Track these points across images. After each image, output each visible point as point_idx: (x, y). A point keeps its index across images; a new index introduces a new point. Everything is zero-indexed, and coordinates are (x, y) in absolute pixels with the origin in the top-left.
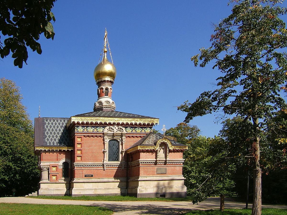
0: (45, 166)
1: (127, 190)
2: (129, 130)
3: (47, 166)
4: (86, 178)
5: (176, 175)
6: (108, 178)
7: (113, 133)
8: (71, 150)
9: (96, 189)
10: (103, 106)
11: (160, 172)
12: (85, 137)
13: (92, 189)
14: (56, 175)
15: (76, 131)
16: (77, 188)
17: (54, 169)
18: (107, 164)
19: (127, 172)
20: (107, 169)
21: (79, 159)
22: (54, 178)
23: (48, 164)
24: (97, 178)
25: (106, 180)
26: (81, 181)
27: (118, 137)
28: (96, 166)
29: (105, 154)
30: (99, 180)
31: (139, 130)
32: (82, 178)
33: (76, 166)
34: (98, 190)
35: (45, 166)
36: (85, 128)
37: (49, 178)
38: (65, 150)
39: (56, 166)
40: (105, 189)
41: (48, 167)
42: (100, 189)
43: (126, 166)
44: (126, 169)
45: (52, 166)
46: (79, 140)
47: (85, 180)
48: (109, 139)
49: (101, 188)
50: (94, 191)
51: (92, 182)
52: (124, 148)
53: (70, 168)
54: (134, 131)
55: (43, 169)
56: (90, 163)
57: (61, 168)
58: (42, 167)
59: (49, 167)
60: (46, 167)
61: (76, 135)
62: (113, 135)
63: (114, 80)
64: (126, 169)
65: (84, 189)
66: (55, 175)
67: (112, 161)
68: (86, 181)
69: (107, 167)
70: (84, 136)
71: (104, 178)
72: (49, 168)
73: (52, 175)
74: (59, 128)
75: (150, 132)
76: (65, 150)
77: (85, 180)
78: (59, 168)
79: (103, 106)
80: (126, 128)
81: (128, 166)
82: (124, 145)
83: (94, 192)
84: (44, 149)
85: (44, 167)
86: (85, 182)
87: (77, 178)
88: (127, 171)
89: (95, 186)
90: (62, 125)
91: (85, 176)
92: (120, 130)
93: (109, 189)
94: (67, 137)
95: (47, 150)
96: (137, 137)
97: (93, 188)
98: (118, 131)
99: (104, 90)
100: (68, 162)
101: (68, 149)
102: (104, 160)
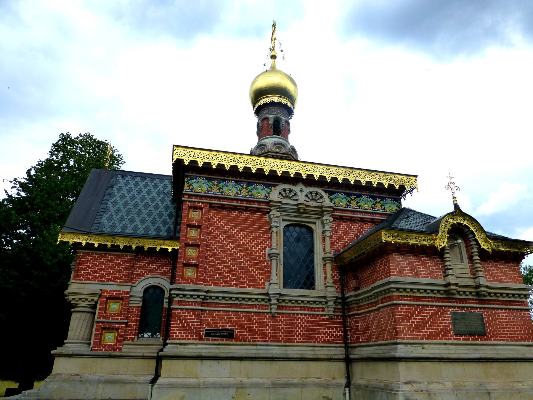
1: (349, 390)
2: (341, 201)
3: (90, 298)
4: (208, 340)
5: (518, 343)
6: (282, 344)
7: (298, 205)
8: (173, 249)
10: (270, 153)
11: (463, 329)
12: (213, 207)
14: (118, 329)
15: (186, 187)
16: (172, 380)
17: (114, 306)
18: (281, 295)
19: (345, 327)
20: (279, 311)
21: (190, 273)
22: (110, 337)
23: (96, 288)
24: (247, 343)
25: (276, 350)
26: (191, 351)
27: (310, 218)
28: (244, 299)
29: (274, 262)
30: (252, 351)
31: (366, 204)
32: (193, 339)
33: (178, 295)
34: (248, 391)
35: (84, 297)
37: (90, 340)
38: (155, 248)
39: (122, 299)
40: (275, 385)
41: (93, 300)
43: (339, 307)
44: (341, 314)
45: (109, 298)
46: (195, 215)
47: (205, 348)
48: (284, 220)
49: (261, 380)
51: (229, 355)
52: (328, 249)
53: (165, 305)
54: (353, 204)
55: (75, 306)
56: (225, 289)
57: (137, 305)
58: (74, 299)
59: (96, 298)
60: (86, 299)
61: (187, 201)
62: (300, 210)
63: (293, 105)
64: (341, 314)
65: (197, 386)
66: (113, 329)
67: (294, 288)
68: (209, 351)
69: (281, 305)
70: (210, 204)
71: (269, 343)
72: (96, 303)
73: (104, 329)
74: (154, 194)
75: (396, 210)
76: (155, 248)
77: (205, 348)
78: (130, 305)
79: (270, 153)
81: (346, 307)
82: (328, 240)
83: (233, 398)
84: (88, 242)
85: (80, 299)
86: (204, 355)
87: (176, 341)
88: (344, 322)
89: (240, 372)
90: (162, 189)
91: (209, 334)
92: (314, 197)
94: (170, 216)
95: (96, 246)
96: (362, 220)
97: (232, 381)
98: (309, 200)
100: (163, 287)
101: (165, 247)
102: (269, 281)
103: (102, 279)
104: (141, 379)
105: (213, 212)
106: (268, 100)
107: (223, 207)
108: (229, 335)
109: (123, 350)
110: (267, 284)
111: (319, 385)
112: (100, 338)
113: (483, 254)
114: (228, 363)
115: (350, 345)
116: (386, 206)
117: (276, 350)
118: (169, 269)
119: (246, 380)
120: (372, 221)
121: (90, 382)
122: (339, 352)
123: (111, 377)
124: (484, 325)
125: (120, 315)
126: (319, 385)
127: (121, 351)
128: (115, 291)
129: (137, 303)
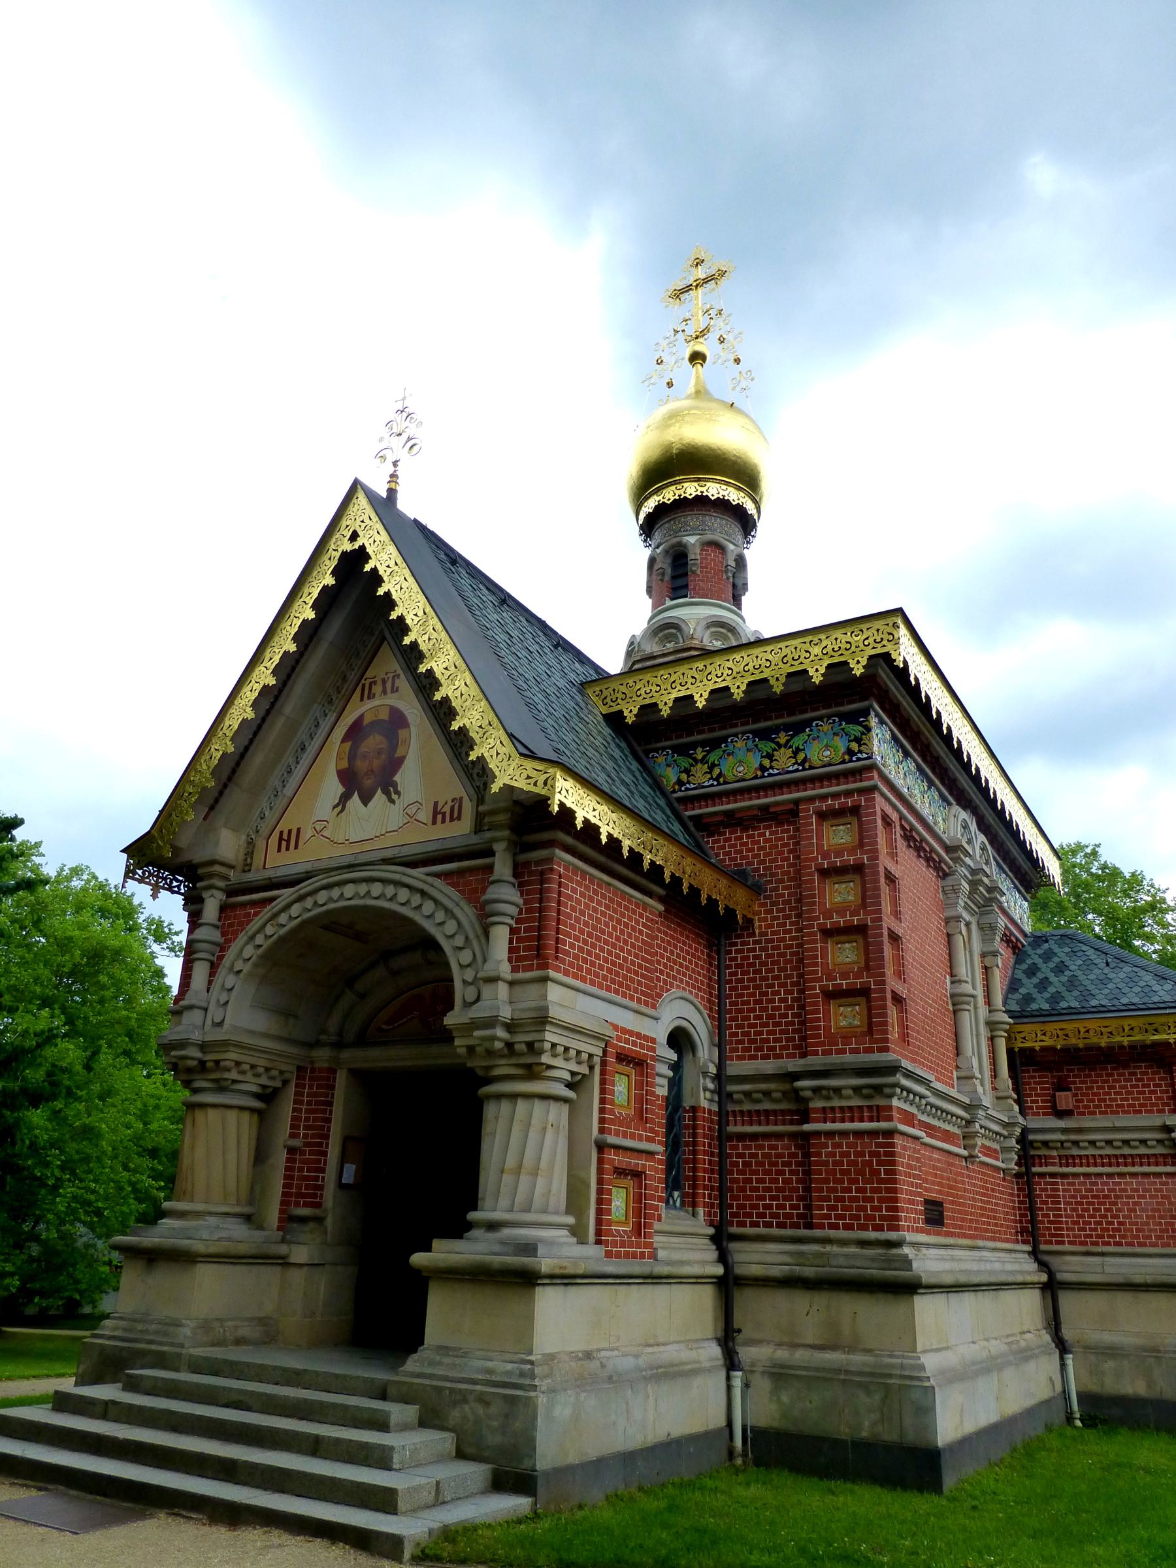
0: (576, 1044)
35: (576, 1044)
106: (691, 489)
109: (661, 1254)
115: (1043, 1247)
122: (1020, 1264)
127: (653, 1256)
128: (631, 1033)
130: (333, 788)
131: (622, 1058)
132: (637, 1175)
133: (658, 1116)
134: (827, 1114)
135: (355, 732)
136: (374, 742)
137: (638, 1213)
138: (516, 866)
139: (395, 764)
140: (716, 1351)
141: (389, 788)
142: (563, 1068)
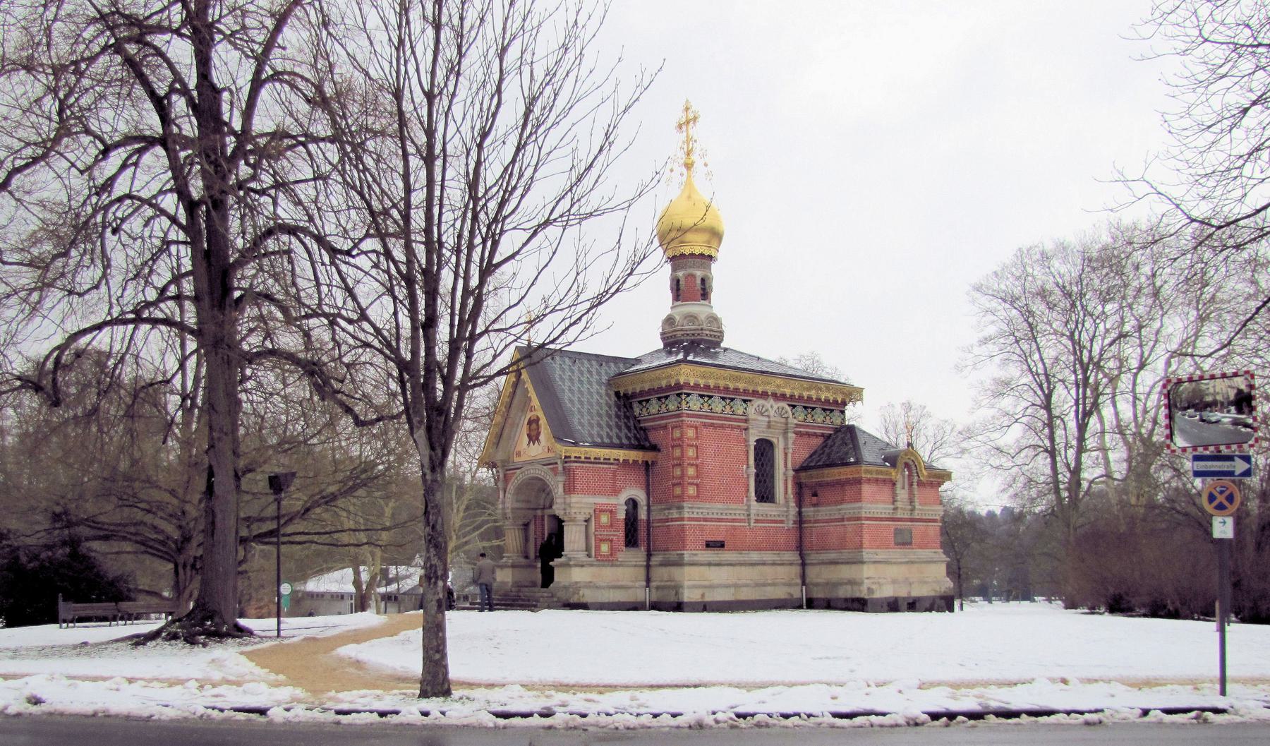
0: (583, 511)
9: (736, 586)
13: (728, 586)
35: (583, 511)
36: (706, 399)
39: (611, 512)
42: (746, 586)
50: (732, 590)
80: (794, 407)
91: (709, 545)
93: (764, 585)
99: (699, 282)
103: (594, 493)
104: (637, 584)
105: (705, 431)
107: (712, 425)
108: (721, 545)
110: (745, 499)
111: (785, 584)
112: (598, 548)
113: (920, 484)
114: (726, 568)
116: (834, 419)
117: (755, 556)
118: (643, 479)
119: (740, 582)
120: (823, 435)
121: (603, 588)
122: (793, 556)
123: (613, 583)
124: (911, 537)
125: (611, 525)
126: (785, 584)
129: (622, 515)
130: (526, 439)
131: (602, 511)
132: (611, 541)
133: (622, 526)
134: (672, 520)
135: (530, 423)
136: (534, 426)
137: (612, 549)
138: (564, 468)
139: (539, 434)
140: (644, 583)
141: (537, 439)
142: (581, 517)
